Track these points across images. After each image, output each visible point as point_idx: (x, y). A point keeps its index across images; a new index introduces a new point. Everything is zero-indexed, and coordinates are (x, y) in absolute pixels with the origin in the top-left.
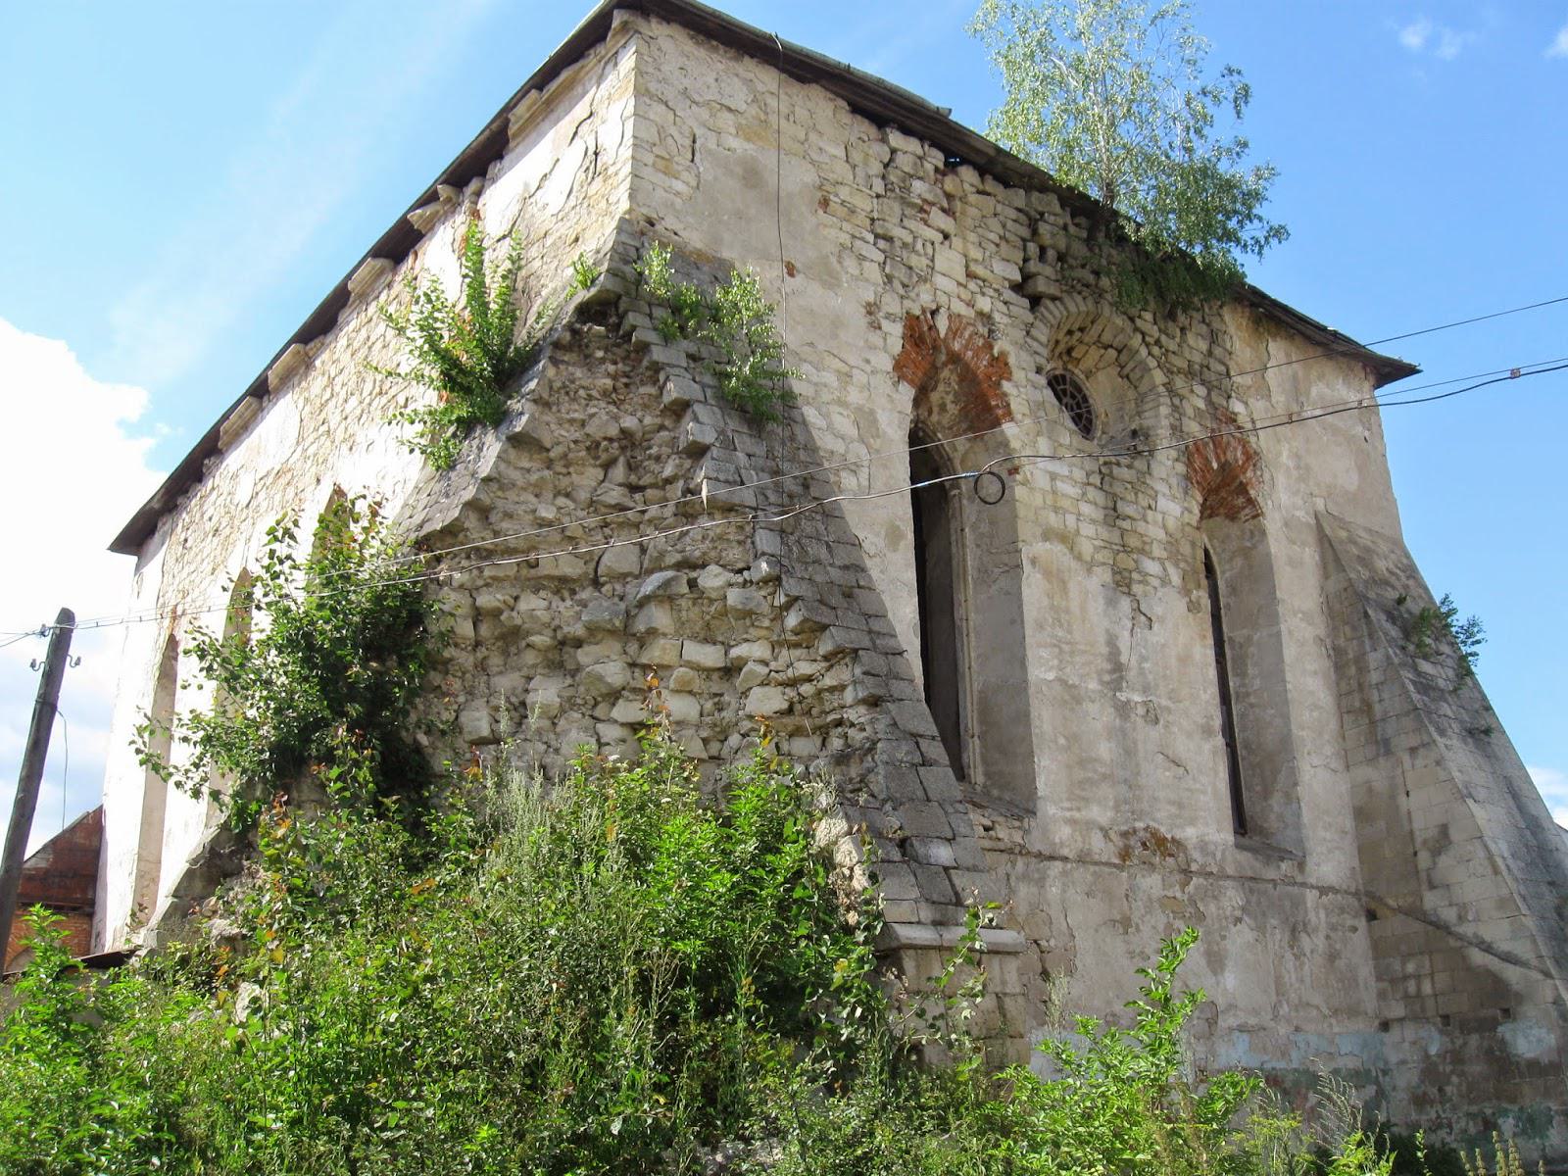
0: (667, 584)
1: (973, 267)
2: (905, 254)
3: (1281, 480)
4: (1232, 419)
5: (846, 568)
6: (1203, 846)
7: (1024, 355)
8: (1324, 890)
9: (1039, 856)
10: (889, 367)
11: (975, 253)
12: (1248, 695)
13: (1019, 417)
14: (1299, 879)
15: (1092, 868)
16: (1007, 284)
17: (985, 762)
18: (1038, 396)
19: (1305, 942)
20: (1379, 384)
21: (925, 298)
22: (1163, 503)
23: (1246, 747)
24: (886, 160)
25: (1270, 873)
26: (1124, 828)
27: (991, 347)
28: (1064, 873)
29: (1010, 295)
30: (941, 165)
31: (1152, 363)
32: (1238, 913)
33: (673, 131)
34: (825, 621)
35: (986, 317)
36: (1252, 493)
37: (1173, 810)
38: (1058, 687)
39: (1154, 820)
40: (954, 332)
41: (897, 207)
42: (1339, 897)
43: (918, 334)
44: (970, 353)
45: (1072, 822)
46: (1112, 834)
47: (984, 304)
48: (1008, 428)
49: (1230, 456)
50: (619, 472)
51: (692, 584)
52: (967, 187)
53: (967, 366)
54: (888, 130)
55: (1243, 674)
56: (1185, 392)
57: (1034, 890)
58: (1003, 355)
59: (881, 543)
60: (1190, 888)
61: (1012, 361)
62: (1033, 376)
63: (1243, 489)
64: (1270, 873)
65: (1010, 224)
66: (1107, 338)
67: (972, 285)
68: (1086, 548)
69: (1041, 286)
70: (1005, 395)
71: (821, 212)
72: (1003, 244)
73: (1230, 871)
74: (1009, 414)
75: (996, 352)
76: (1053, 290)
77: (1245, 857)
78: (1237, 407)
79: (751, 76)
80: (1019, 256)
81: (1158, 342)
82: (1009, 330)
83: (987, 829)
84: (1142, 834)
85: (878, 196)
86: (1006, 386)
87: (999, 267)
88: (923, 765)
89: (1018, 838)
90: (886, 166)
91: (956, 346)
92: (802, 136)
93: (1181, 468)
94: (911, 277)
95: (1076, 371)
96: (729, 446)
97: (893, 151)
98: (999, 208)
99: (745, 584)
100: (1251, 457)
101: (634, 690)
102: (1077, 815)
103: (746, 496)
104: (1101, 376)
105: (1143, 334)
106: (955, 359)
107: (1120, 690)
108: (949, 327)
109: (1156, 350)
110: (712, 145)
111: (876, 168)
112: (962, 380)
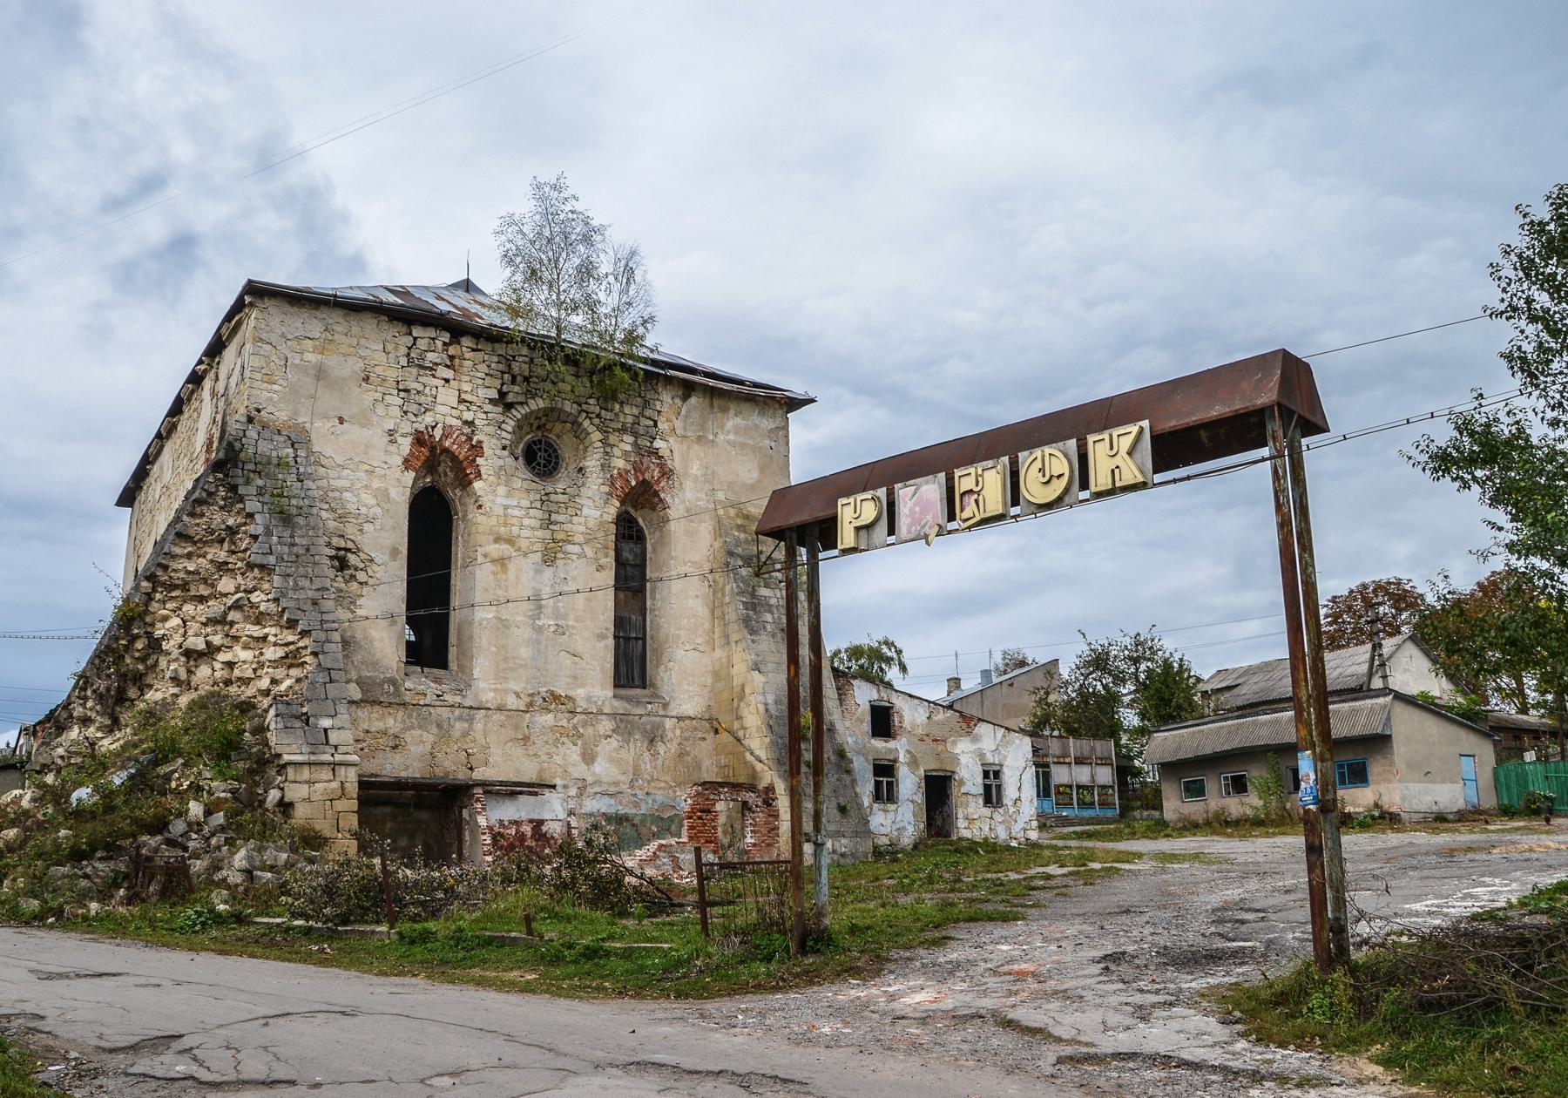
0: (238, 600)
1: (463, 396)
2: (417, 397)
3: (688, 484)
4: (655, 453)
5: (318, 590)
6: (589, 699)
7: (494, 441)
8: (680, 719)
9: (471, 708)
11: (467, 387)
12: (655, 610)
13: (484, 477)
14: (661, 712)
15: (505, 713)
16: (487, 401)
17: (458, 659)
18: (501, 462)
19: (661, 748)
20: (788, 412)
21: (428, 419)
22: (585, 511)
23: (652, 638)
24: (410, 345)
25: (640, 711)
26: (531, 692)
27: (471, 439)
28: (487, 716)
29: (488, 407)
30: (447, 341)
31: (591, 429)
32: (609, 733)
33: (274, 358)
34: (298, 618)
35: (470, 423)
36: (662, 495)
37: (570, 680)
38: (494, 620)
40: (445, 436)
41: (414, 371)
42: (694, 722)
43: (419, 439)
44: (455, 446)
45: (495, 690)
46: (522, 695)
47: (468, 416)
48: (477, 485)
49: (647, 476)
50: (226, 545)
51: (248, 599)
52: (464, 349)
53: (453, 453)
54: (412, 327)
55: (653, 599)
56: (616, 443)
57: (466, 725)
58: (480, 442)
59: (386, 558)
61: (485, 445)
62: (498, 452)
63: (656, 494)
64: (640, 711)
65: (493, 365)
66: (563, 417)
67: (462, 407)
68: (524, 544)
69: (510, 398)
70: (478, 465)
71: (364, 384)
72: (488, 378)
73: (606, 711)
74: (479, 475)
75: (474, 443)
76: (521, 399)
77: (616, 703)
78: (658, 444)
79: (325, 316)
80: (497, 383)
81: (599, 416)
82: (485, 428)
83: (438, 696)
84: (544, 694)
85: (403, 367)
86: (479, 461)
87: (482, 392)
88: (331, 682)
89: (458, 699)
90: (410, 348)
91: (447, 444)
92: (355, 343)
93: (606, 489)
94: (420, 410)
95: (550, 436)
96: (268, 533)
97: (415, 339)
98: (486, 357)
99: (268, 600)
100: (667, 473)
101: (227, 647)
102: (499, 686)
103: (272, 560)
104: (565, 437)
105: (587, 412)
106: (446, 451)
107: (539, 619)
108: (443, 434)
109: (596, 421)
110: (297, 361)
111: (404, 350)
112: (452, 461)
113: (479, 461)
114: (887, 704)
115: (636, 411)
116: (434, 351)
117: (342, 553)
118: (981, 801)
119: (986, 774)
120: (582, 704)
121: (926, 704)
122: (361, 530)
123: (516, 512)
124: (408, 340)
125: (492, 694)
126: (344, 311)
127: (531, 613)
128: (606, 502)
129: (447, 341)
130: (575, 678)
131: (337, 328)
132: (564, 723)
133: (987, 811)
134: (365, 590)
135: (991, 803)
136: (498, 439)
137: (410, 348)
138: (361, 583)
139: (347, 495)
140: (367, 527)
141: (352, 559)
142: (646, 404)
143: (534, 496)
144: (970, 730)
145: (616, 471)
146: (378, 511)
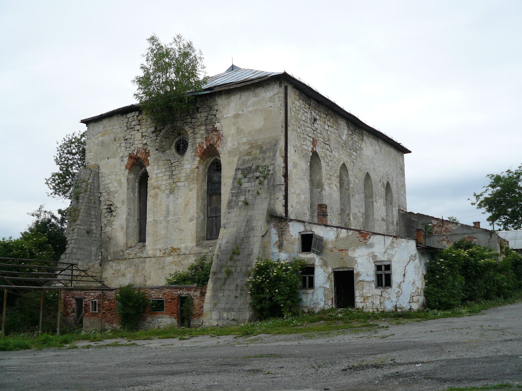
3: (230, 139)
9: (145, 258)
10: (124, 168)
26: (165, 248)
28: (150, 260)
29: (151, 135)
36: (218, 149)
38: (153, 221)
39: (174, 245)
43: (131, 157)
60: (180, 258)
63: (215, 148)
67: (143, 139)
68: (163, 187)
71: (115, 142)
74: (148, 165)
78: (217, 125)
80: (154, 125)
86: (149, 158)
90: (127, 123)
105: (186, 123)
107: (168, 217)
109: (190, 125)
111: (125, 124)
113: (149, 158)
114: (311, 233)
115: (206, 114)
116: (134, 121)
117: (110, 206)
118: (373, 286)
119: (379, 268)
120: (183, 251)
121: (335, 229)
122: (114, 197)
123: (160, 175)
124: (126, 120)
125: (152, 251)
127: (166, 215)
128: (194, 160)
129: (137, 115)
130: (181, 240)
131: (107, 125)
132: (176, 259)
133: (378, 291)
134: (115, 217)
135: (382, 286)
136: (154, 147)
137: (127, 123)
138: (114, 216)
139: (110, 185)
140: (116, 195)
141: (112, 208)
142: (211, 108)
143: (167, 166)
144: (365, 241)
145: (198, 145)
146: (118, 188)
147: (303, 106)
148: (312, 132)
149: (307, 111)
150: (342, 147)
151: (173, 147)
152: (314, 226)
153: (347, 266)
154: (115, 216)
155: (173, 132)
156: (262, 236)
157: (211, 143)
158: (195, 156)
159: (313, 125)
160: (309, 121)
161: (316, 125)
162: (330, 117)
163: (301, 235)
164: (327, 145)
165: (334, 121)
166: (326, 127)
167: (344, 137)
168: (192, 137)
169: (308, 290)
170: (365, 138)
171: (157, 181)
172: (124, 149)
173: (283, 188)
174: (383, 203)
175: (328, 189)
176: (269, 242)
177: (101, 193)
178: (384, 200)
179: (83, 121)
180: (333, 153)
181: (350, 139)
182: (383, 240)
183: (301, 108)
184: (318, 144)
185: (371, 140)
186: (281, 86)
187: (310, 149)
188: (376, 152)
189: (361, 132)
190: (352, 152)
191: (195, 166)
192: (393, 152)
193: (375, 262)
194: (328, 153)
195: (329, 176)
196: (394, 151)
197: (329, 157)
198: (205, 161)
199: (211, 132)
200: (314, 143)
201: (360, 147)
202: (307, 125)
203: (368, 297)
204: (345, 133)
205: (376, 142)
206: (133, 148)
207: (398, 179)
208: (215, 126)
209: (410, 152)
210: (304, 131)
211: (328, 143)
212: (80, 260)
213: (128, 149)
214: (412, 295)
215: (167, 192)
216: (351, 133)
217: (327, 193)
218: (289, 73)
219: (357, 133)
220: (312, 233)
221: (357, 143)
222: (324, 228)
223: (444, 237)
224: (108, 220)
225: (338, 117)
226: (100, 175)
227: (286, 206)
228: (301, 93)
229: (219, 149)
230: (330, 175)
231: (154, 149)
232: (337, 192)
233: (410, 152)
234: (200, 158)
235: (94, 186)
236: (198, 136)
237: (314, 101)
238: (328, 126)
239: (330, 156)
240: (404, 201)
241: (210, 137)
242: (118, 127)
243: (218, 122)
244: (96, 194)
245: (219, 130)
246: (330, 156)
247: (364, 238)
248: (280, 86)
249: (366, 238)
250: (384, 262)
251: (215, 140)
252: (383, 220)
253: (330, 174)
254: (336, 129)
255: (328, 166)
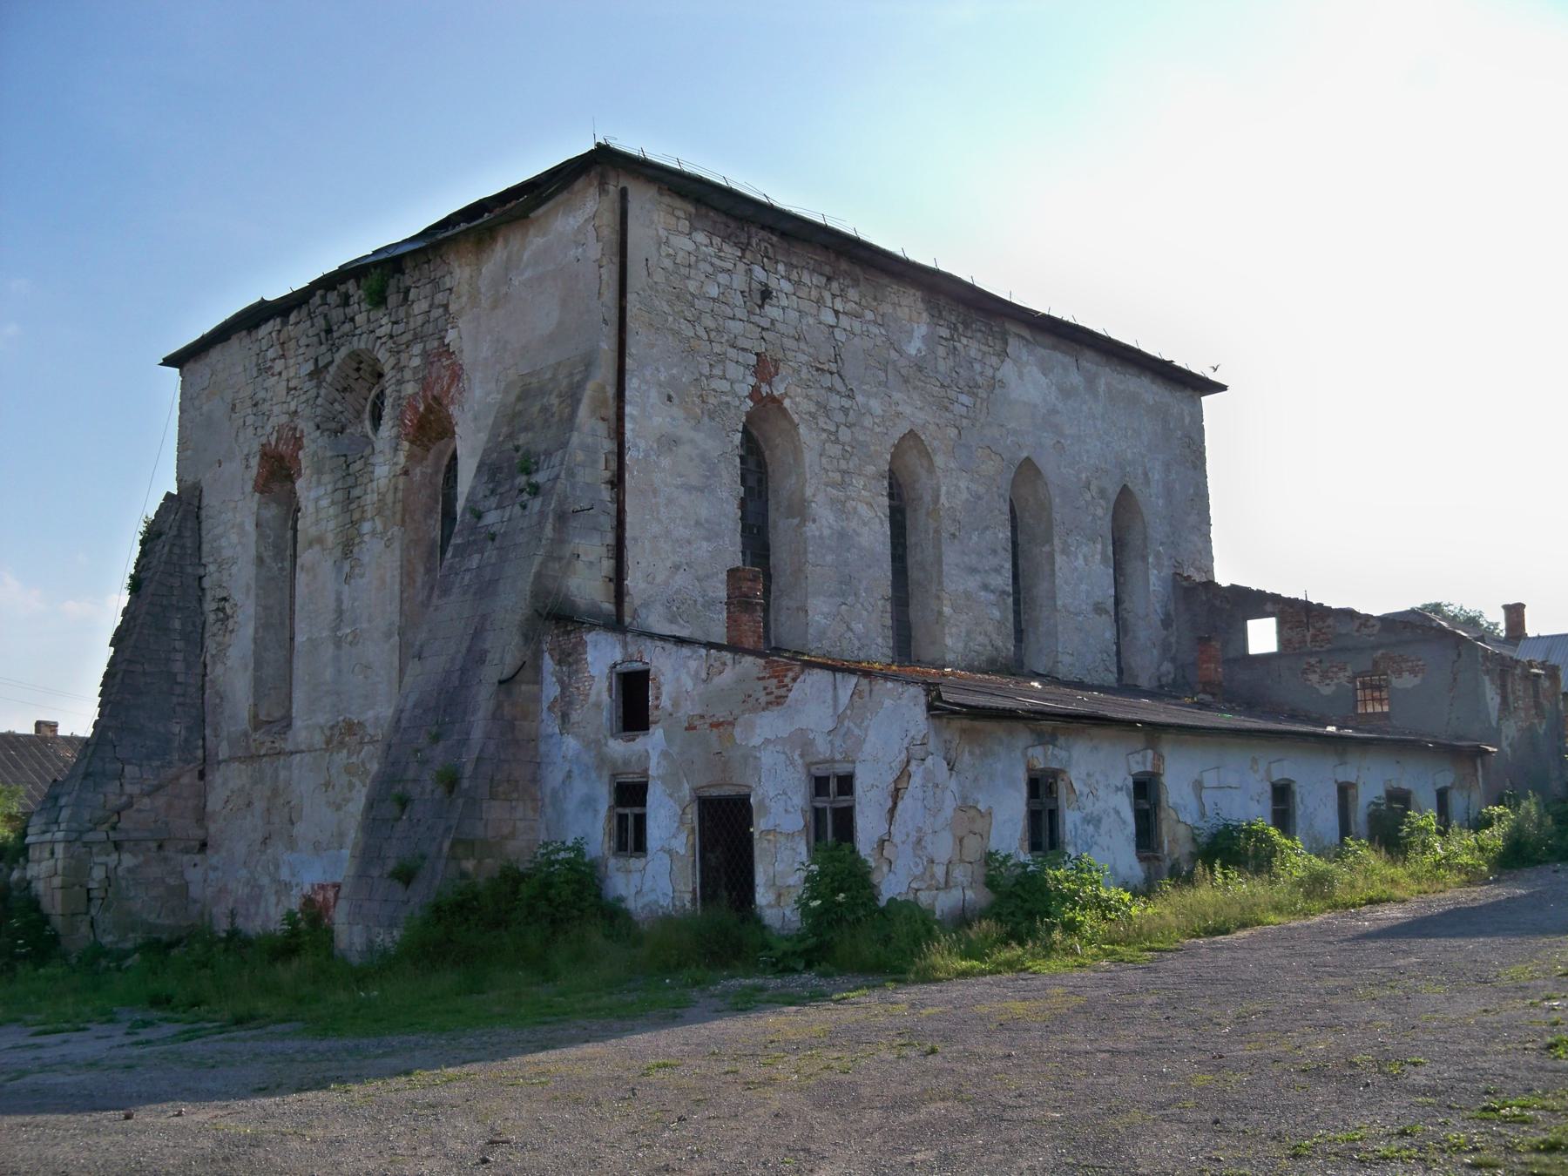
26: (331, 723)
36: (451, 409)
67: (289, 399)
74: (300, 475)
102: (309, 722)
107: (339, 629)
116: (272, 346)
119: (820, 785)
121: (703, 652)
122: (230, 575)
126: (219, 347)
134: (233, 635)
142: (436, 284)
144: (783, 692)
147: (711, 250)
148: (758, 336)
149: (730, 266)
150: (906, 381)
151: (367, 415)
152: (648, 642)
153: (731, 778)
154: (232, 632)
155: (358, 370)
156: (501, 682)
157: (435, 393)
158: (398, 437)
159: (758, 311)
160: (739, 300)
161: (771, 311)
162: (848, 282)
163: (619, 675)
164: (832, 373)
165: (862, 296)
166: (829, 318)
167: (914, 347)
168: (394, 380)
169: (632, 860)
170: (1014, 345)
171: (317, 522)
172: (250, 431)
173: (608, 522)
174: (1098, 557)
175: (831, 519)
176: (537, 699)
177: (205, 566)
178: (1104, 546)
179: (169, 361)
180: (860, 398)
181: (941, 351)
182: (830, 688)
183: (701, 257)
184: (783, 370)
185: (1042, 352)
186: (604, 190)
187: (744, 389)
188: (1067, 393)
189: (997, 329)
190: (952, 394)
191: (398, 469)
192: (1150, 391)
193: (808, 766)
194: (835, 401)
195: (837, 477)
196: (1154, 387)
197: (840, 417)
198: (428, 450)
199: (436, 359)
200: (764, 368)
201: (993, 378)
202: (729, 312)
203: (789, 886)
204: (916, 334)
205: (1068, 360)
206: (268, 429)
207: (1173, 476)
208: (447, 341)
209: (1222, 388)
210: (713, 334)
211: (833, 367)
212: (130, 764)
213: (260, 431)
214: (914, 885)
215: (338, 552)
216: (945, 333)
217: (827, 532)
218: (628, 143)
219: (979, 335)
220: (645, 667)
221: (977, 367)
222: (675, 648)
223: (1313, 661)
224: (219, 644)
225: (885, 280)
226: (203, 513)
227: (618, 577)
228: (703, 211)
229: (453, 410)
230: (844, 472)
231: (311, 425)
232: (877, 527)
233: (1222, 388)
234: (412, 442)
235: (183, 547)
236: (408, 374)
237: (763, 233)
238: (837, 313)
239: (845, 411)
240: (1200, 546)
241: (434, 376)
242: (240, 369)
243: (452, 328)
244: (189, 570)
245: (453, 352)
246: (845, 411)
247: (779, 682)
248: (603, 190)
249: (787, 680)
250: (837, 766)
251: (446, 381)
252: (1098, 609)
253: (845, 467)
254: (875, 322)
255: (837, 441)
